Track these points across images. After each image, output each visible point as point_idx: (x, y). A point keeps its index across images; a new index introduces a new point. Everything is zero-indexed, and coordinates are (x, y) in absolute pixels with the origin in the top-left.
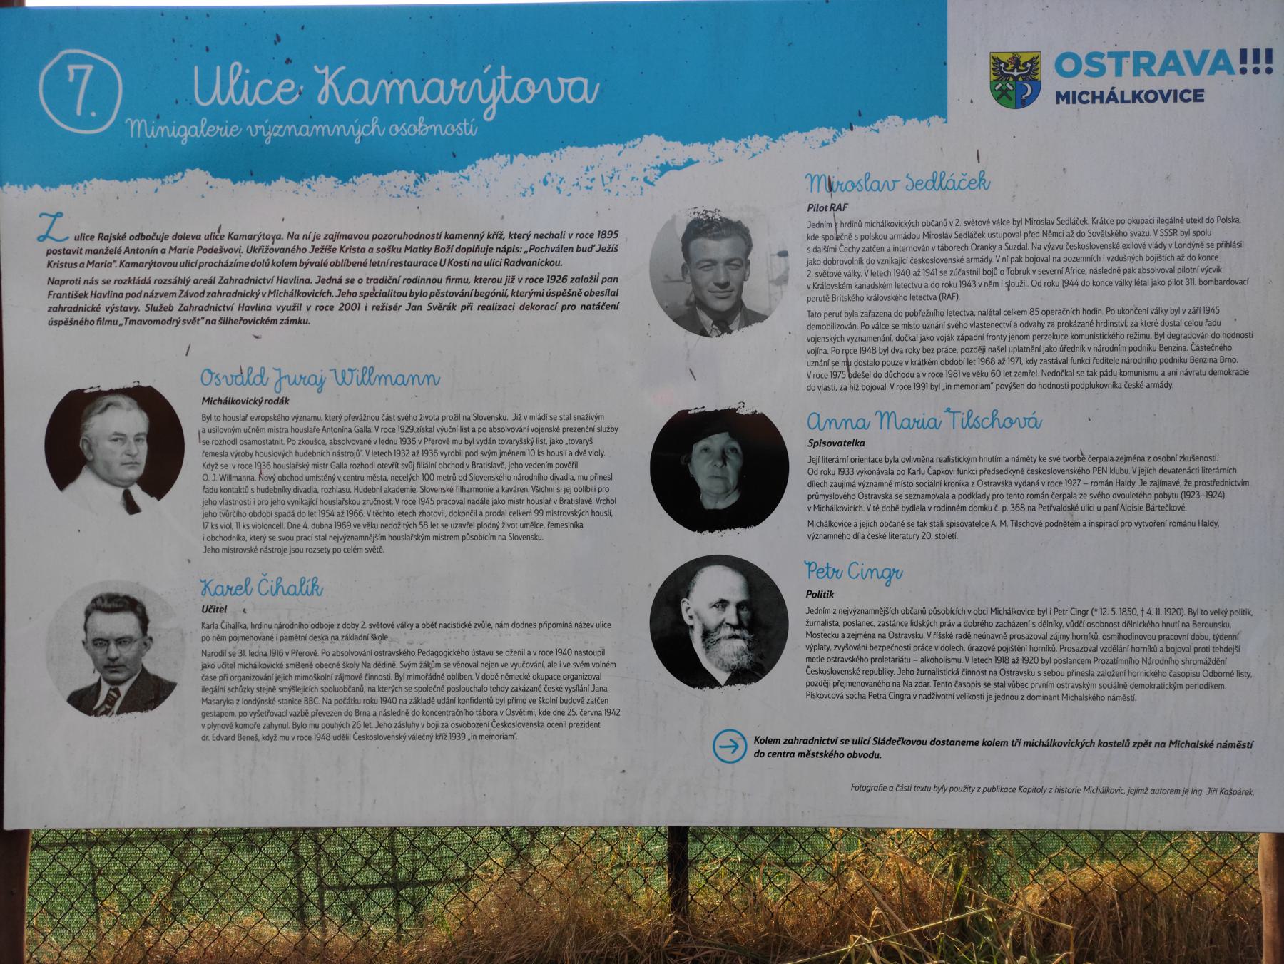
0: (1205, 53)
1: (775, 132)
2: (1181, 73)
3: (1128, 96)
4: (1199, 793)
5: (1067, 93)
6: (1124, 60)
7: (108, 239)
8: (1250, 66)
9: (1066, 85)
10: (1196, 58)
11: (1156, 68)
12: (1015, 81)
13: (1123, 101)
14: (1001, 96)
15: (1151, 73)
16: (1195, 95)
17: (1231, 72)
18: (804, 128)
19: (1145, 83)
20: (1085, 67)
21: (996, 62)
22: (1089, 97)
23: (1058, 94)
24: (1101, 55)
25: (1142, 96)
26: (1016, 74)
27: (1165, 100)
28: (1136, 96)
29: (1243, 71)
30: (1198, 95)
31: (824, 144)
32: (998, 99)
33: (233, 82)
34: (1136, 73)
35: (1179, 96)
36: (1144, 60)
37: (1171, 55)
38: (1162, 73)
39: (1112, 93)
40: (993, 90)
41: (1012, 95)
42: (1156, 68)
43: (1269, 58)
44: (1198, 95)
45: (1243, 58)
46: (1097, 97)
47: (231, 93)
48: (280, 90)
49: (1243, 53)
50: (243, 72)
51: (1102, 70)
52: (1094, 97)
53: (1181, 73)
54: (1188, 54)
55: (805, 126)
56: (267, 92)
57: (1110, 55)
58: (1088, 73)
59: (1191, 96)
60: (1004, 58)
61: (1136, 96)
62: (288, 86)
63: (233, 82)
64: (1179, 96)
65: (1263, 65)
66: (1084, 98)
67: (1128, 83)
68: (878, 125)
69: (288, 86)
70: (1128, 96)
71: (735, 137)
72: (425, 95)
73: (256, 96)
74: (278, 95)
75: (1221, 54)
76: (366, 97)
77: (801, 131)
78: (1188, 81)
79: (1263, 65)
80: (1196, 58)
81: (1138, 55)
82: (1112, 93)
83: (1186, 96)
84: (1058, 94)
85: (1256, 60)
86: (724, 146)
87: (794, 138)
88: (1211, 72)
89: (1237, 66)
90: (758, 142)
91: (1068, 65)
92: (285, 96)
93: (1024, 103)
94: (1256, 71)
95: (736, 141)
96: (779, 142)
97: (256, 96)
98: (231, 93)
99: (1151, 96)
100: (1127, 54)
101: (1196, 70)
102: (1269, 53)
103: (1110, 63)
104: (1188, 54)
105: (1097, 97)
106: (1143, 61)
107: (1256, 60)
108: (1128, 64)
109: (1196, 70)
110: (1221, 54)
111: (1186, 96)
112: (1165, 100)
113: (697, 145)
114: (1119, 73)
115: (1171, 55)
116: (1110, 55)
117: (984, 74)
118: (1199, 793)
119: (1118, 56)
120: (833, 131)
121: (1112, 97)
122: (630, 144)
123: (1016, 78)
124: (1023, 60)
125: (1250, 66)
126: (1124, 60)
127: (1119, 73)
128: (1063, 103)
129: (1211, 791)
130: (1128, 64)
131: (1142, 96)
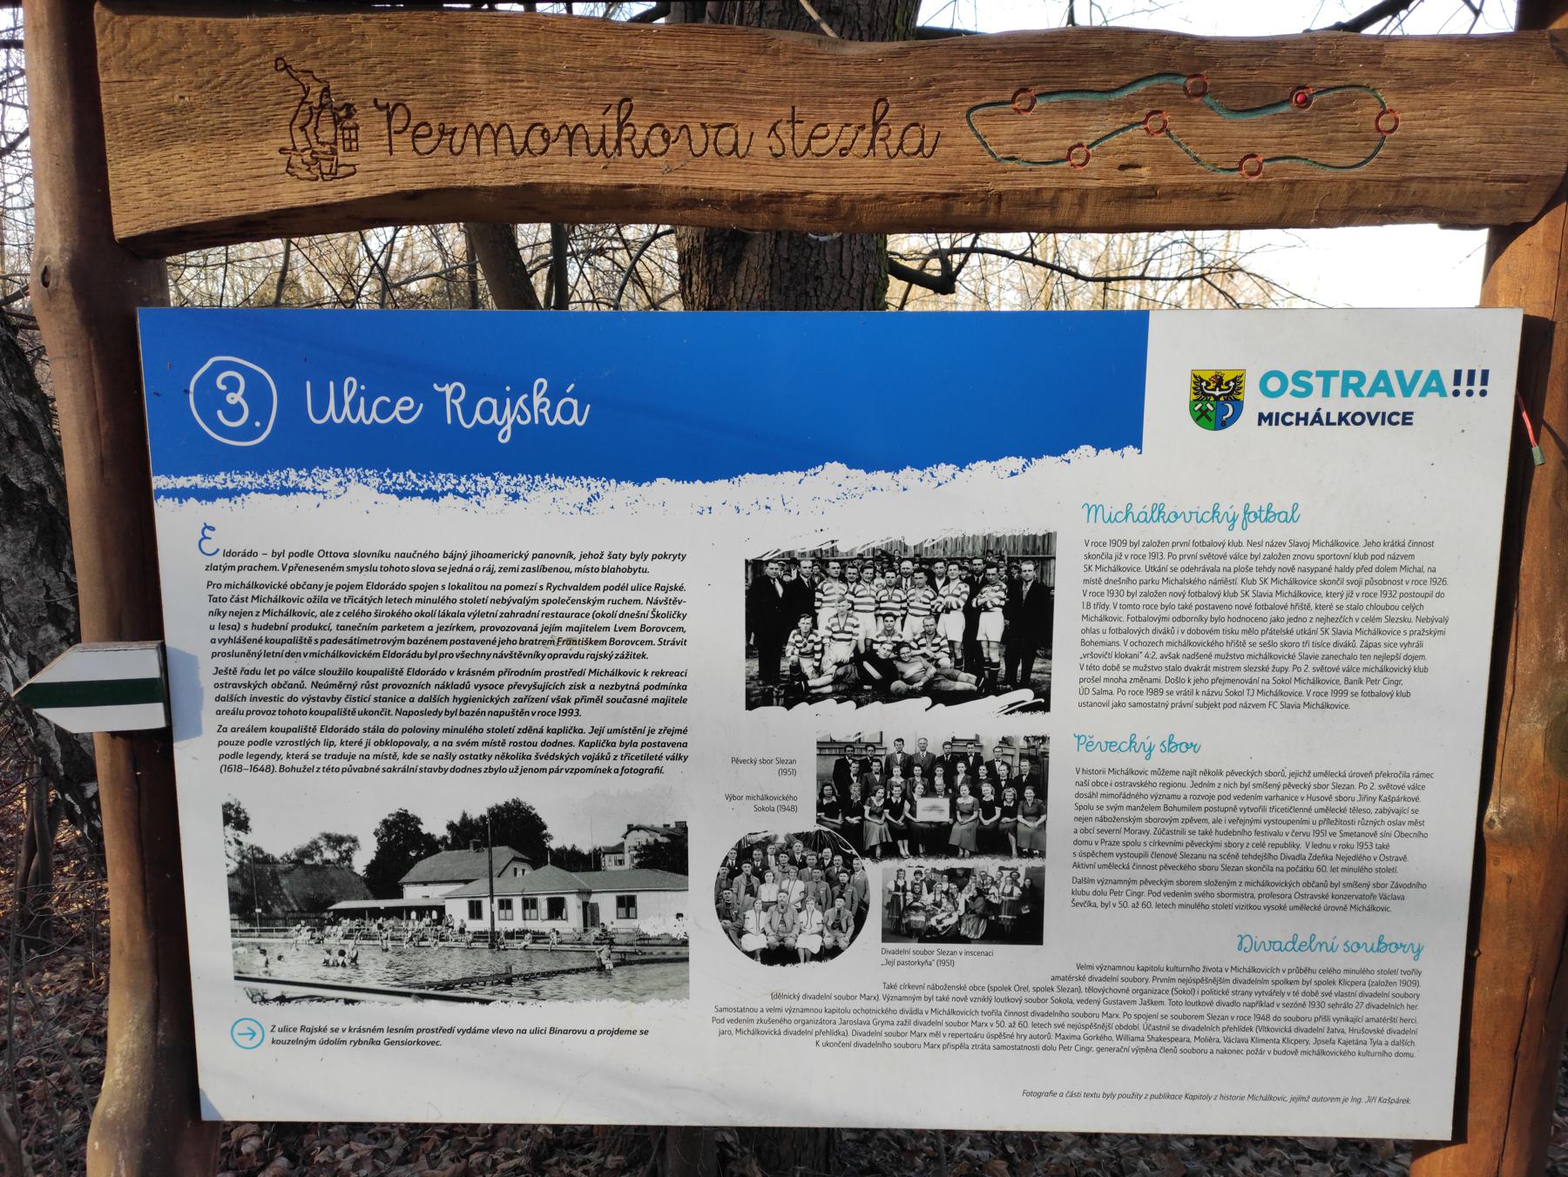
0: (1418, 374)
1: (962, 460)
2: (1391, 394)
3: (1334, 419)
5: (1270, 415)
6: (1333, 380)
7: (665, 589)
8: (1464, 387)
9: (1269, 406)
10: (1408, 381)
11: (1365, 389)
12: (1216, 401)
13: (1328, 423)
14: (1201, 417)
15: (1359, 394)
16: (1404, 418)
17: (1443, 394)
18: (993, 456)
19: (1352, 404)
20: (1291, 387)
21: (1198, 380)
22: (1293, 419)
23: (1261, 416)
24: (1308, 374)
25: (1349, 418)
26: (1217, 393)
27: (1372, 422)
28: (1342, 419)
29: (1456, 393)
30: (1407, 419)
31: (1013, 474)
32: (1197, 420)
33: (348, 399)
34: (1344, 394)
35: (1387, 419)
36: (1353, 380)
37: (1383, 375)
38: (1371, 394)
39: (1317, 415)
40: (1192, 410)
41: (1212, 415)
42: (1365, 389)
43: (1484, 381)
44: (1407, 419)
45: (1457, 381)
46: (1301, 419)
47: (347, 410)
48: (398, 408)
49: (1458, 374)
50: (358, 389)
51: (1309, 390)
52: (1298, 419)
53: (1391, 394)
54: (1400, 374)
55: (993, 454)
56: (385, 410)
57: (1319, 374)
58: (1294, 393)
59: (1399, 419)
60: (1206, 377)
61: (1342, 419)
62: (406, 404)
63: (348, 399)
64: (1387, 419)
65: (1477, 387)
66: (1288, 419)
67: (1335, 405)
68: (1069, 455)
69: (406, 404)
70: (1334, 419)
71: (920, 466)
72: (558, 416)
73: (374, 415)
74: (396, 413)
75: (1435, 375)
76: (575, 417)
77: (989, 460)
78: (1399, 404)
79: (1477, 387)
80: (1408, 381)
81: (1347, 374)
82: (1317, 415)
83: (1394, 419)
84: (1261, 416)
85: (1471, 382)
86: (909, 475)
87: (982, 468)
88: (1423, 394)
89: (1450, 387)
90: (945, 470)
91: (1274, 385)
92: (405, 415)
93: (1224, 425)
94: (1470, 393)
95: (921, 469)
96: (966, 471)
97: (374, 415)
98: (347, 410)
99: (1358, 419)
100: (1336, 374)
101: (1407, 392)
102: (1485, 374)
103: (1316, 383)
104: (1400, 374)
105: (1301, 419)
106: (1352, 382)
107: (1471, 382)
108: (1336, 383)
109: (1407, 392)
110: (1435, 375)
111: (1394, 419)
112: (1372, 422)
113: (881, 473)
114: (1326, 393)
115: (1383, 375)
116: (1319, 374)
117: (1185, 393)
119: (1327, 376)
120: (1022, 461)
121: (1317, 419)
122: (811, 471)
123: (1217, 398)
124: (1225, 380)
125: (1464, 387)
126: (1333, 380)
127: (1326, 392)
128: (1265, 425)
130: (1336, 383)
131: (1349, 418)
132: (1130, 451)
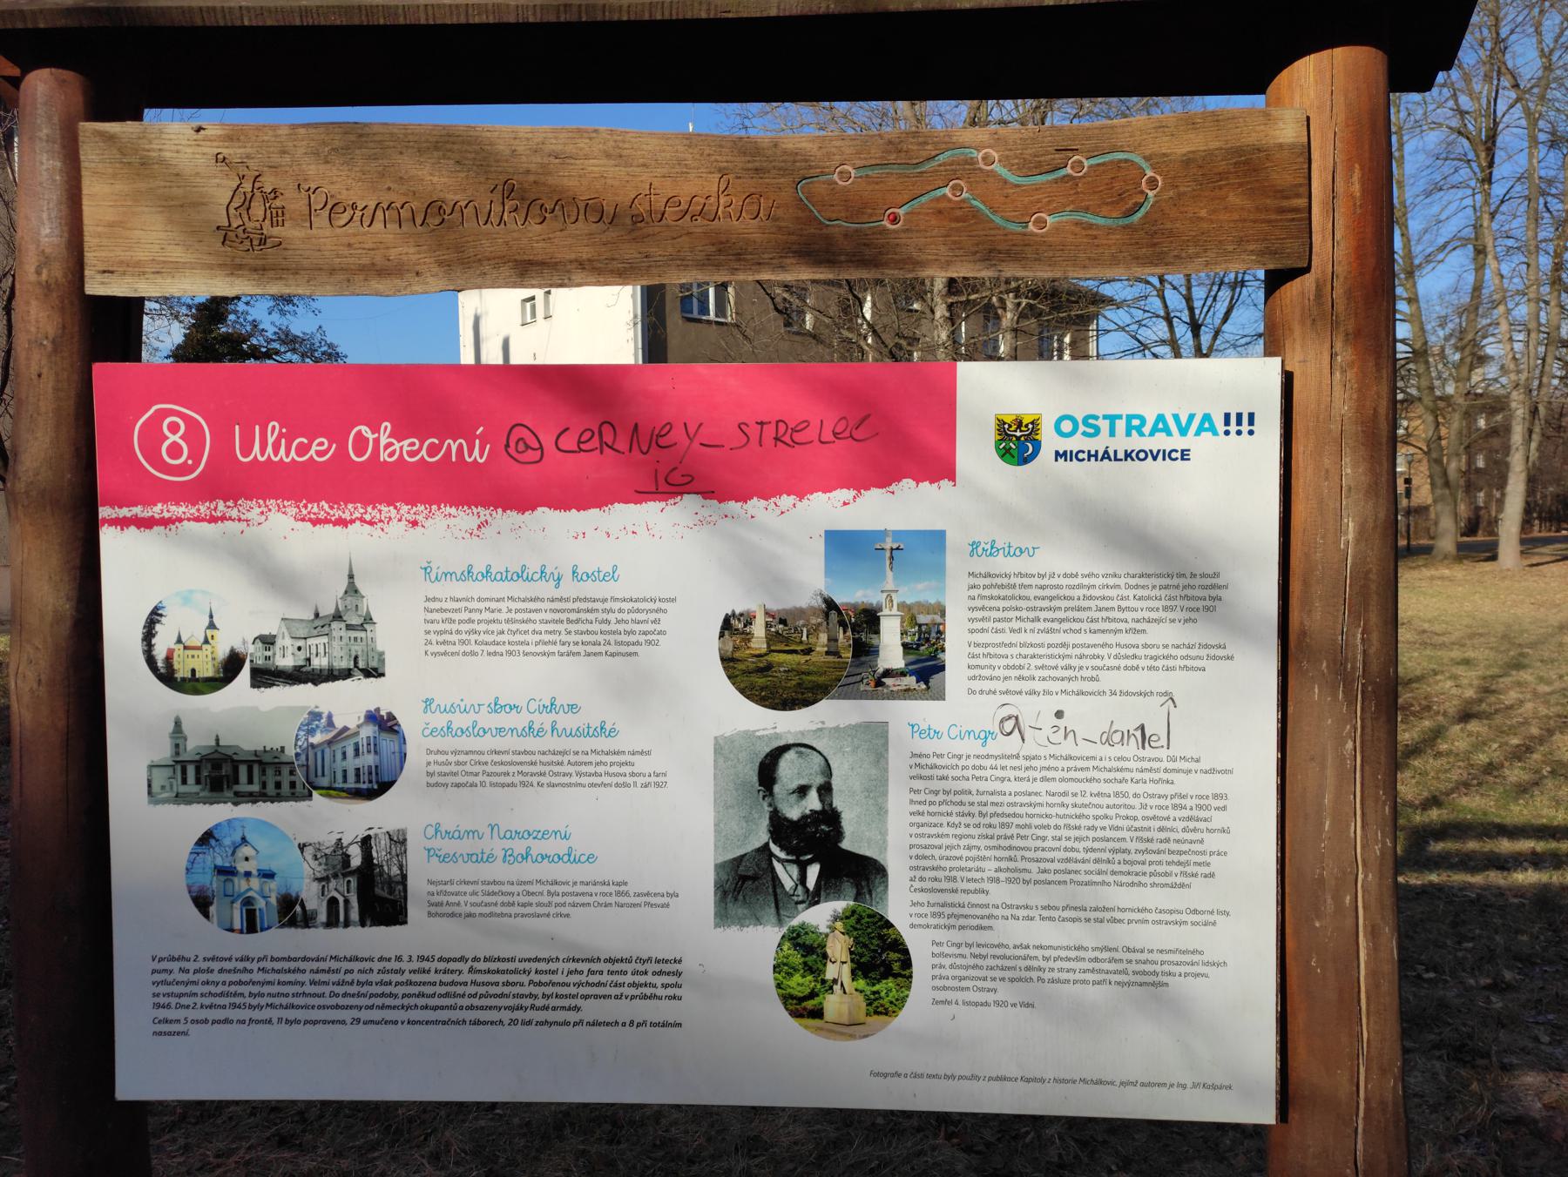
0: (1192, 417)
2: (1169, 433)
3: (1121, 455)
4: (1184, 1087)
8: (1233, 428)
10: (1184, 422)
14: (1005, 454)
15: (1141, 434)
17: (1215, 433)
20: (1082, 428)
21: (1001, 423)
22: (1085, 456)
23: (1057, 453)
24: (1096, 418)
27: (1155, 458)
28: (1128, 455)
29: (1227, 433)
32: (1002, 457)
33: (271, 440)
34: (1128, 434)
35: (1168, 455)
36: (1136, 422)
37: (1161, 418)
38: (1152, 434)
39: (1106, 452)
40: (997, 448)
41: (1015, 453)
42: (1147, 430)
43: (1251, 422)
45: (1227, 423)
47: (270, 450)
48: (314, 448)
49: (1227, 416)
51: (1097, 431)
52: (1090, 456)
53: (1169, 433)
54: (1176, 417)
56: (303, 450)
57: (1105, 417)
58: (1084, 434)
59: (1178, 455)
60: (1008, 420)
61: (1128, 455)
62: (321, 444)
63: (271, 440)
64: (1168, 455)
65: (1245, 428)
66: (1081, 456)
69: (321, 444)
70: (1121, 455)
73: (293, 453)
74: (312, 452)
78: (1176, 442)
79: (1245, 428)
80: (1184, 422)
81: (1130, 417)
82: (1106, 452)
84: (1057, 453)
85: (1239, 423)
88: (1197, 434)
89: (1221, 428)
93: (1025, 461)
94: (1239, 433)
97: (293, 453)
98: (270, 450)
99: (1142, 455)
100: (1120, 417)
101: (1183, 431)
102: (1251, 416)
103: (1104, 425)
104: (1176, 417)
107: (1239, 423)
108: (1121, 425)
109: (1183, 431)
112: (1155, 458)
114: (1112, 433)
115: (1161, 418)
116: (1105, 417)
117: (991, 435)
118: (1184, 1087)
119: (1112, 419)
123: (1018, 438)
125: (1233, 428)
127: (1112, 433)
128: (1061, 461)
129: (1195, 1086)
130: (1121, 425)
132: (945, 483)
